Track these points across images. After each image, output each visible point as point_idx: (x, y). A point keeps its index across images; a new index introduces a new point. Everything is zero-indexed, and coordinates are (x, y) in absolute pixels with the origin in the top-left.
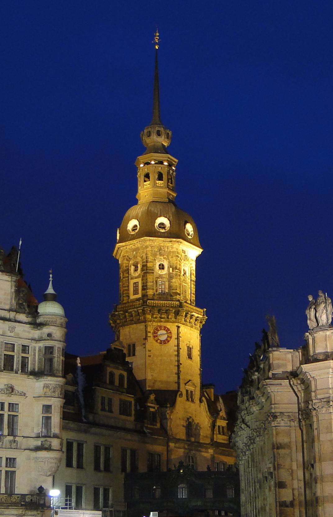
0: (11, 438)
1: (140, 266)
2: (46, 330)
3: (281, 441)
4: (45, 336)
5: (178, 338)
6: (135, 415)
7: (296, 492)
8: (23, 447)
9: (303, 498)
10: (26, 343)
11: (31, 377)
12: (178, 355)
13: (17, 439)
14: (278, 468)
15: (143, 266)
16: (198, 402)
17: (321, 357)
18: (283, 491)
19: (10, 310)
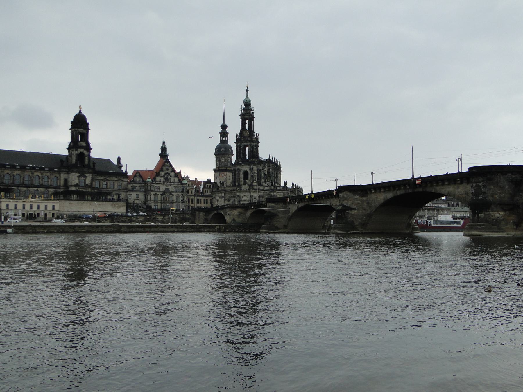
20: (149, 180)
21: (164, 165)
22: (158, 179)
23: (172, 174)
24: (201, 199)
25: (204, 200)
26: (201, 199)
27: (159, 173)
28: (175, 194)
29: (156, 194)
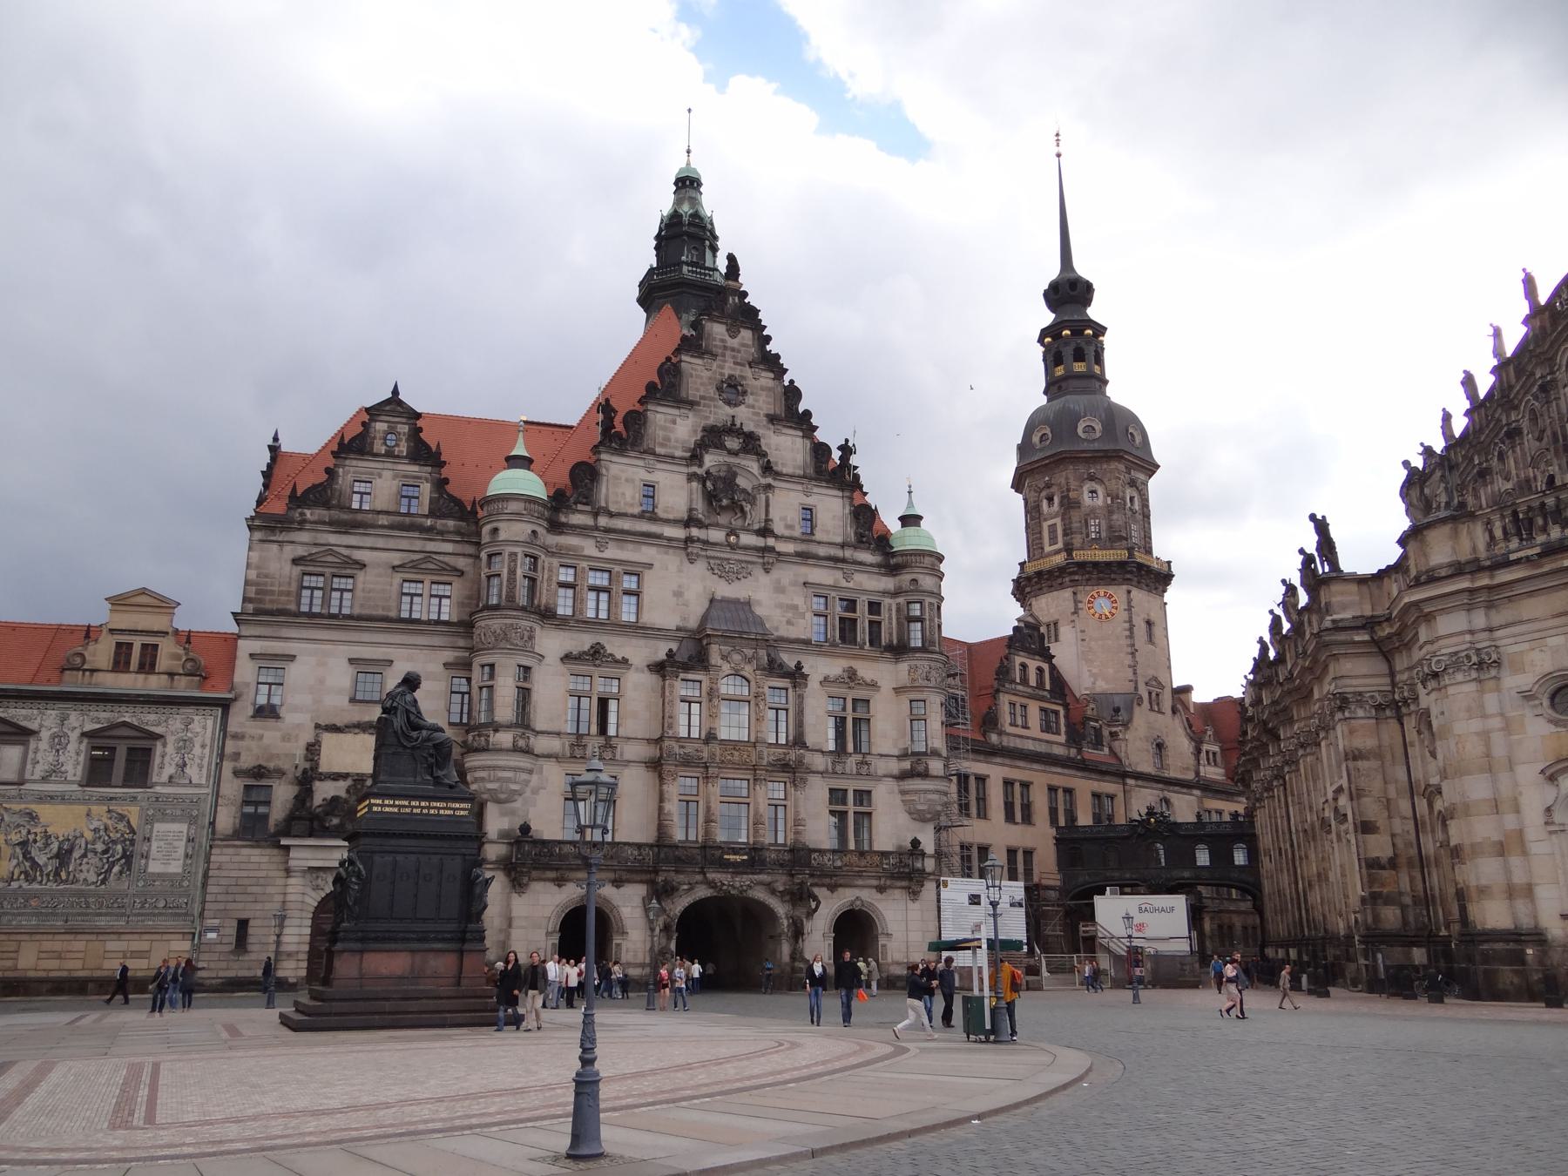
0: (859, 757)
1: (1056, 499)
2: (906, 578)
3: (1360, 746)
4: (906, 585)
5: (1129, 608)
6: (1067, 733)
7: (1399, 841)
8: (880, 772)
9: (1413, 852)
10: (875, 598)
11: (888, 655)
12: (1131, 636)
13: (868, 758)
14: (1359, 797)
15: (1062, 498)
16: (1169, 711)
17: (1443, 573)
18: (1371, 838)
19: (843, 546)
20: (527, 483)
21: (693, 344)
22: (622, 479)
23: (787, 448)
24: (981, 779)
25: (1008, 783)
26: (981, 779)
27: (636, 420)
28: (819, 668)
29: (596, 654)
